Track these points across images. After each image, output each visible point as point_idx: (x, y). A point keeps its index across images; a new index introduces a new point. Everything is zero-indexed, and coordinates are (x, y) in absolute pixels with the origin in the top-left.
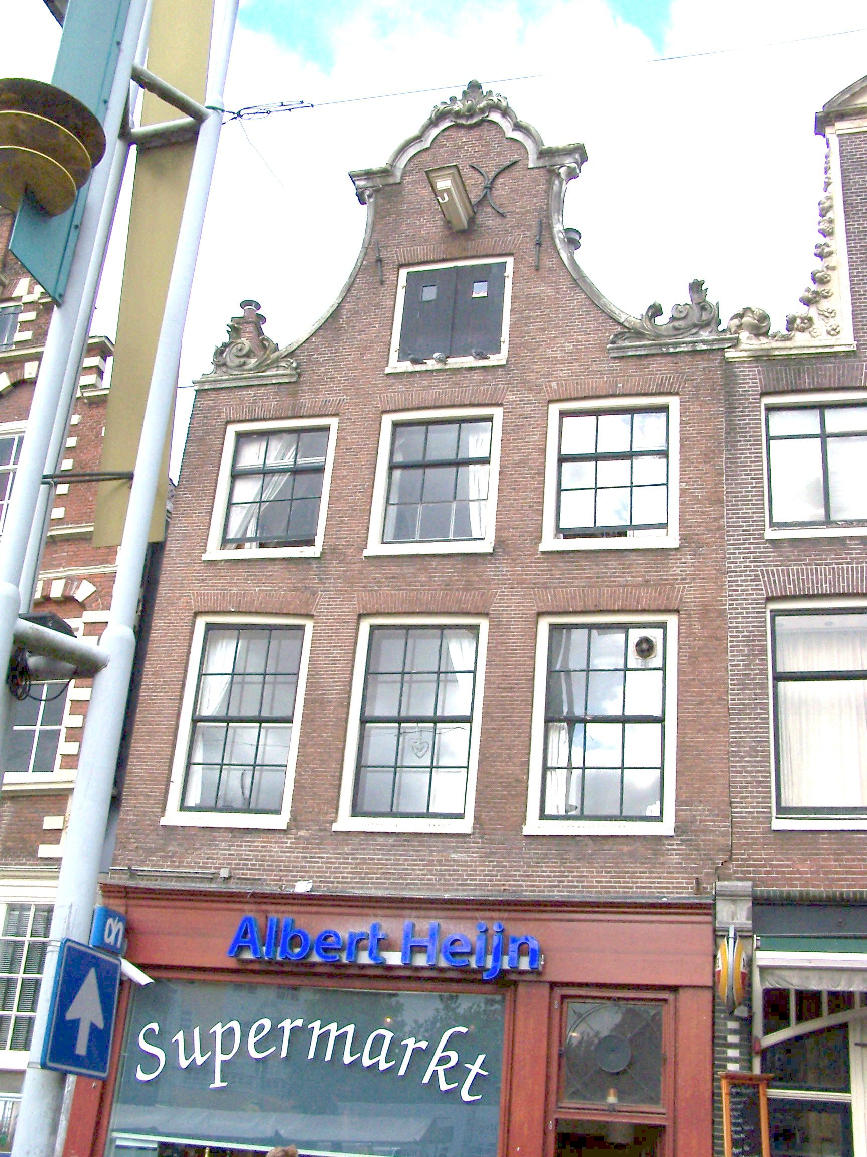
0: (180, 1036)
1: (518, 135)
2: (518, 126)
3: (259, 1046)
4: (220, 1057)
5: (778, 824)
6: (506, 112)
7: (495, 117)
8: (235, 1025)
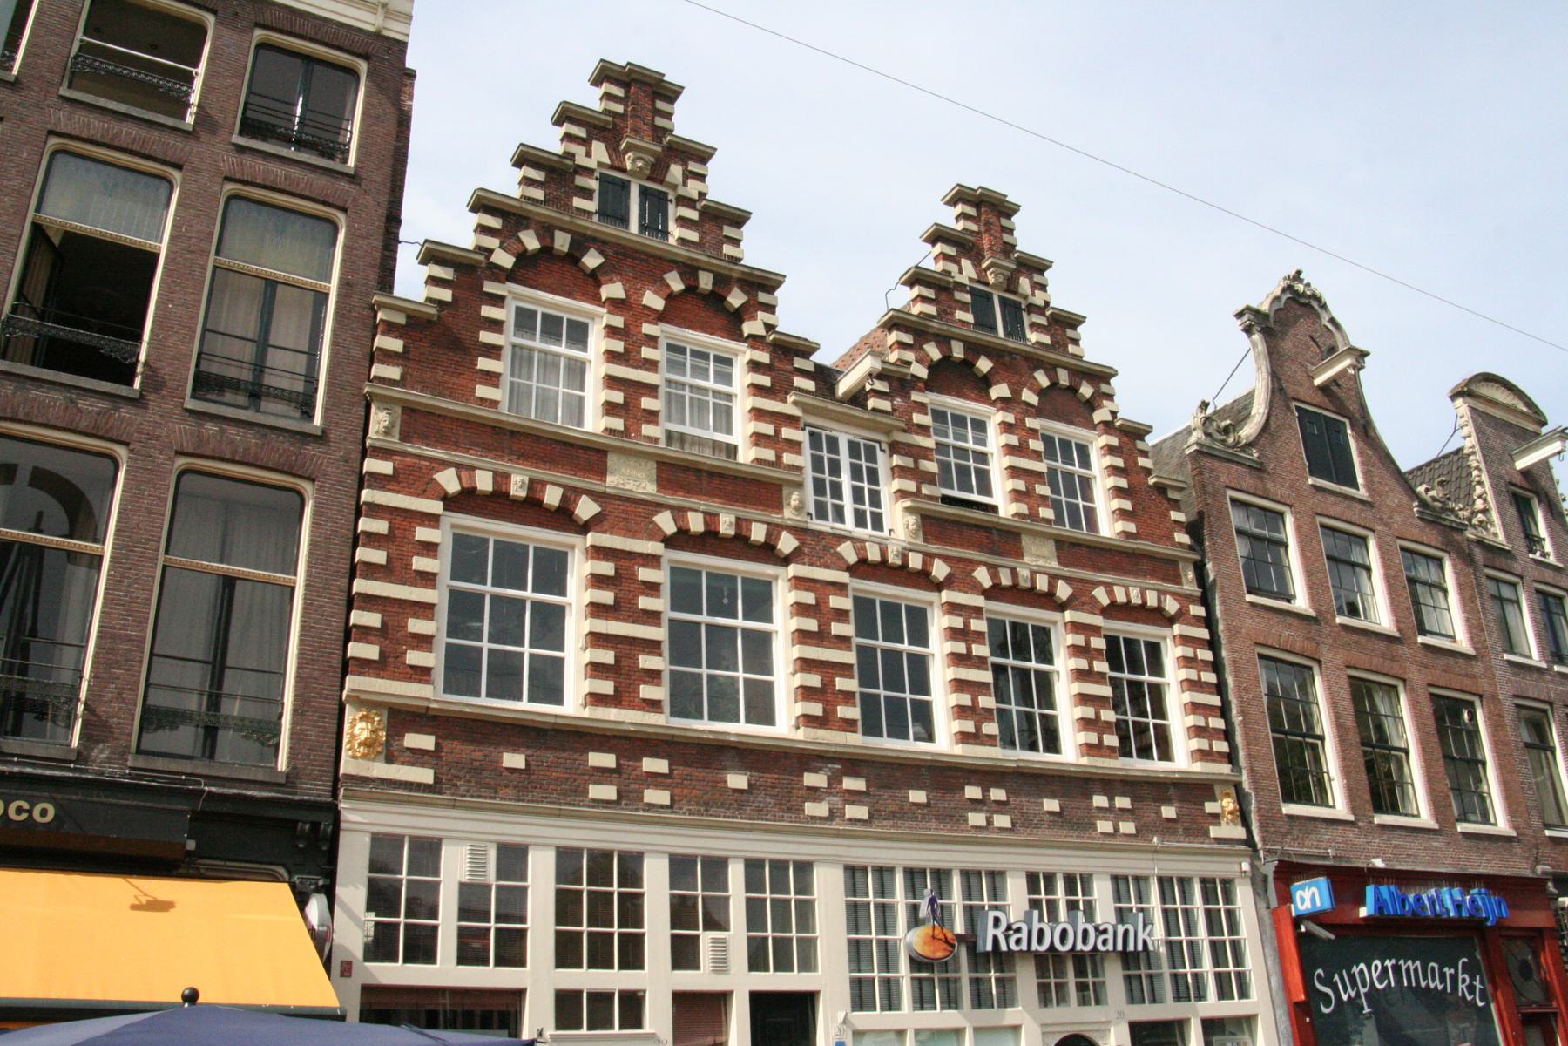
0: (1336, 978)
1: (1329, 326)
2: (1332, 321)
3: (1381, 981)
4: (1363, 991)
5: (1548, 833)
6: (1324, 307)
7: (1315, 304)
8: (1362, 965)
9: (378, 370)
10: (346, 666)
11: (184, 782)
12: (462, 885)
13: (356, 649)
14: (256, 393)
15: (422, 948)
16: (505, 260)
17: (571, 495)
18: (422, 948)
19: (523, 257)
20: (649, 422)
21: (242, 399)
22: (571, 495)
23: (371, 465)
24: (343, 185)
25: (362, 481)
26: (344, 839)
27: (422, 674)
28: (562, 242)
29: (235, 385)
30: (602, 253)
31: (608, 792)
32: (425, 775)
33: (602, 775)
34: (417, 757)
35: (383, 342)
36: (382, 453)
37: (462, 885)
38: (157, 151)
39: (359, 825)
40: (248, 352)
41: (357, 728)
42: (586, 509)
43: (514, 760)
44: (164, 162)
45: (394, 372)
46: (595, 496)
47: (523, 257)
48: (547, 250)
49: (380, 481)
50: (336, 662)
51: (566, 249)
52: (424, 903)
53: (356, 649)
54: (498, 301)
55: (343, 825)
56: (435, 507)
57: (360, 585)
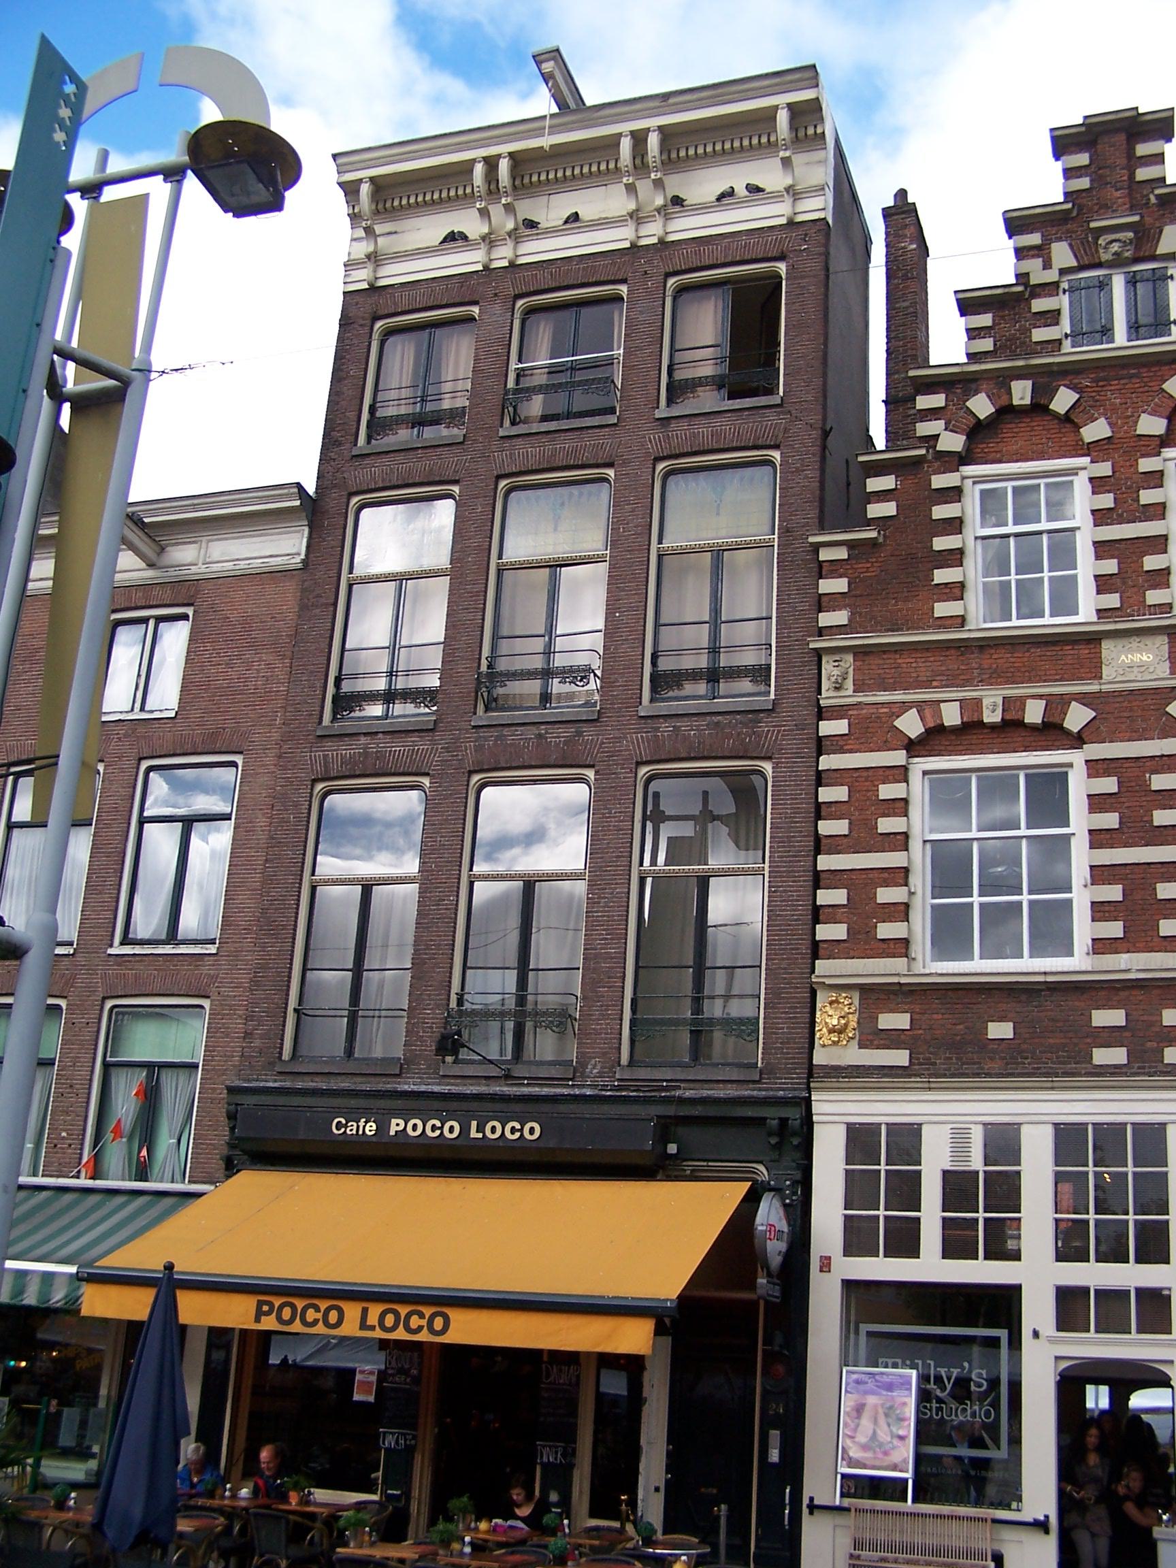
9: (826, 619)
10: (816, 950)
11: (666, 1089)
12: (945, 1173)
13: (825, 932)
14: (713, 675)
15: (904, 1241)
16: (953, 442)
17: (1057, 705)
18: (904, 1241)
19: (978, 431)
20: (1154, 587)
21: (702, 688)
22: (1057, 705)
23: (828, 728)
24: (772, 417)
25: (821, 746)
26: (819, 1132)
27: (901, 947)
28: (1021, 393)
29: (693, 675)
30: (1074, 388)
31: (1116, 1056)
32: (900, 1057)
33: (1110, 1036)
34: (891, 1039)
35: (830, 586)
36: (837, 712)
37: (945, 1173)
38: (586, 457)
39: (834, 1115)
40: (702, 636)
41: (828, 1016)
42: (1077, 717)
43: (1000, 1030)
44: (598, 466)
45: (839, 617)
46: (1085, 699)
47: (978, 431)
48: (1006, 412)
49: (838, 744)
50: (805, 949)
51: (1027, 401)
52: (907, 1190)
53: (825, 932)
54: (955, 494)
55: (815, 1118)
56: (898, 757)
57: (825, 862)
